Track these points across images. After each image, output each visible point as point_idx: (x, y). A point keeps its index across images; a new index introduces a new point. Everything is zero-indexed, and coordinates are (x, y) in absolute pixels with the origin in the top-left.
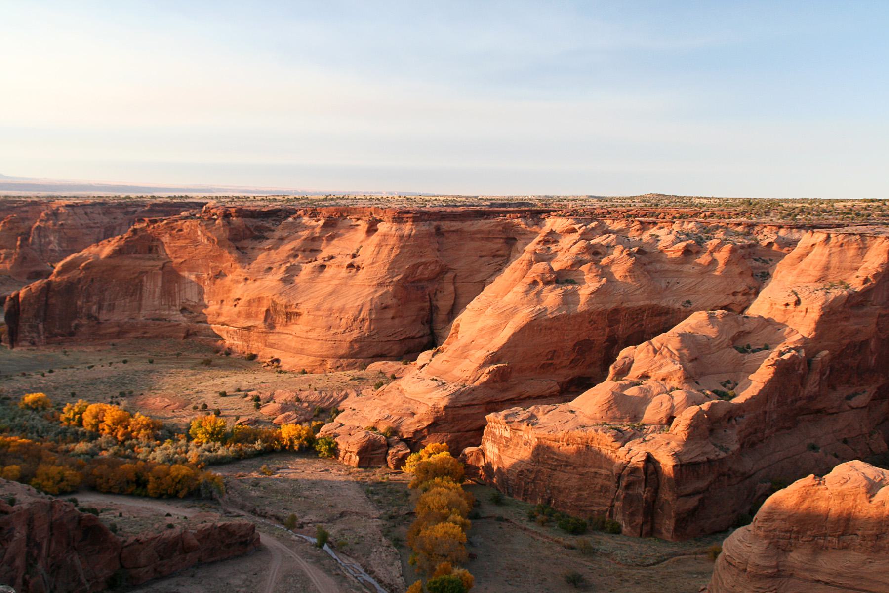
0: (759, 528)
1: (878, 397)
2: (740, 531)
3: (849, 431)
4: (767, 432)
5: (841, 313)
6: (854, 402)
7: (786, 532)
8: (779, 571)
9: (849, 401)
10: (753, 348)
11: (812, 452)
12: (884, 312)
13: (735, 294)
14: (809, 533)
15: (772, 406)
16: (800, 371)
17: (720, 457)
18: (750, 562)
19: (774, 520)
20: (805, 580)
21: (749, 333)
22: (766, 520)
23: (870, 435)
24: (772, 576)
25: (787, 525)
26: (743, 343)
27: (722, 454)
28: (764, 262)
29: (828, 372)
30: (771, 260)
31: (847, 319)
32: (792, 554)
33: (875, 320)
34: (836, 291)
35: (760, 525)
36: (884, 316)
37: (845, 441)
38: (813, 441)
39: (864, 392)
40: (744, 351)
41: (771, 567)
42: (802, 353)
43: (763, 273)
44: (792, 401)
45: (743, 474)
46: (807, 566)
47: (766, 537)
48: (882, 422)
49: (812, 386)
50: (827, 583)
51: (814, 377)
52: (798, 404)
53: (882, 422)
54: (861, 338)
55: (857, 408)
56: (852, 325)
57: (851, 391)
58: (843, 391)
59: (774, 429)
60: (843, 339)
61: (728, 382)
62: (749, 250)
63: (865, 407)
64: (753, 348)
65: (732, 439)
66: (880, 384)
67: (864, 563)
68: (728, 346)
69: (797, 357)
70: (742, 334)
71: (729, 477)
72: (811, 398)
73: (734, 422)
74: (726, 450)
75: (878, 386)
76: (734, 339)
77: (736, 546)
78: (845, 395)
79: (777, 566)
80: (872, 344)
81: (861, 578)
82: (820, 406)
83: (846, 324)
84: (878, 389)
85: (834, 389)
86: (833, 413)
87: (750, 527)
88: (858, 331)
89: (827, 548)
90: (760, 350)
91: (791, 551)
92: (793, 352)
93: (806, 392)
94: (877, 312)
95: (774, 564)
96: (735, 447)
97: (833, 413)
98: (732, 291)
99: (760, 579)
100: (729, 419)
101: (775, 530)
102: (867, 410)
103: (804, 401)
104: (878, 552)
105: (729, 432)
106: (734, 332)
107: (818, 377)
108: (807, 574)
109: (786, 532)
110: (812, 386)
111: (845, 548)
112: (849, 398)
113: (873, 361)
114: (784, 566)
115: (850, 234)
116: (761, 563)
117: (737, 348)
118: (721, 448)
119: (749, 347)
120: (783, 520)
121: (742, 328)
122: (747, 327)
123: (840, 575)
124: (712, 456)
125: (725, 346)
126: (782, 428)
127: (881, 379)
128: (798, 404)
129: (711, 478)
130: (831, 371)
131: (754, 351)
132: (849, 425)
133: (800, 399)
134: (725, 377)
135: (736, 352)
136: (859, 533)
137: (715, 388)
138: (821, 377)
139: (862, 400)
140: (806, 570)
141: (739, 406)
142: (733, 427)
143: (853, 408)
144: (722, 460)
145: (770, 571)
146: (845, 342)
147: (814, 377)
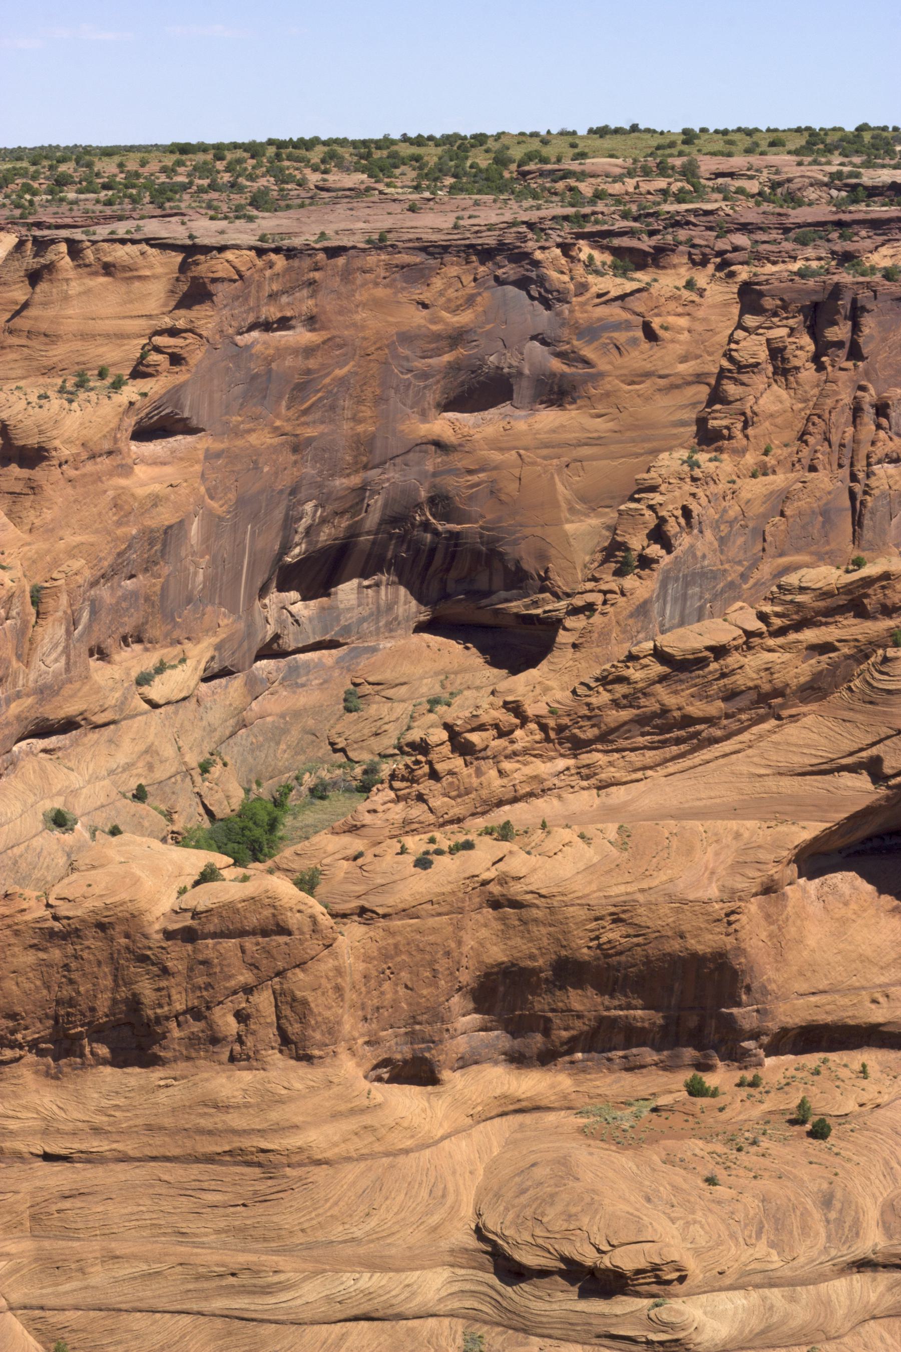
3: (150, 767)
5: (110, 453)
6: (157, 691)
9: (145, 689)
11: (57, 833)
12: (219, 446)
23: (205, 768)
29: (85, 616)
36: (218, 455)
37: (140, 795)
38: (58, 803)
39: (183, 661)
48: (233, 734)
49: (48, 662)
53: (233, 734)
54: (165, 516)
57: (150, 661)
60: (119, 524)
66: (222, 634)
72: (45, 692)
75: (215, 640)
78: (134, 674)
80: (195, 529)
82: (70, 709)
83: (123, 482)
84: (219, 647)
88: (156, 501)
93: (32, 676)
102: (193, 700)
103: (30, 701)
107: (61, 631)
112: (143, 680)
113: (200, 577)
127: (223, 622)
128: (15, 708)
130: (94, 612)
132: (146, 752)
133: (18, 696)
138: (68, 633)
143: (155, 705)
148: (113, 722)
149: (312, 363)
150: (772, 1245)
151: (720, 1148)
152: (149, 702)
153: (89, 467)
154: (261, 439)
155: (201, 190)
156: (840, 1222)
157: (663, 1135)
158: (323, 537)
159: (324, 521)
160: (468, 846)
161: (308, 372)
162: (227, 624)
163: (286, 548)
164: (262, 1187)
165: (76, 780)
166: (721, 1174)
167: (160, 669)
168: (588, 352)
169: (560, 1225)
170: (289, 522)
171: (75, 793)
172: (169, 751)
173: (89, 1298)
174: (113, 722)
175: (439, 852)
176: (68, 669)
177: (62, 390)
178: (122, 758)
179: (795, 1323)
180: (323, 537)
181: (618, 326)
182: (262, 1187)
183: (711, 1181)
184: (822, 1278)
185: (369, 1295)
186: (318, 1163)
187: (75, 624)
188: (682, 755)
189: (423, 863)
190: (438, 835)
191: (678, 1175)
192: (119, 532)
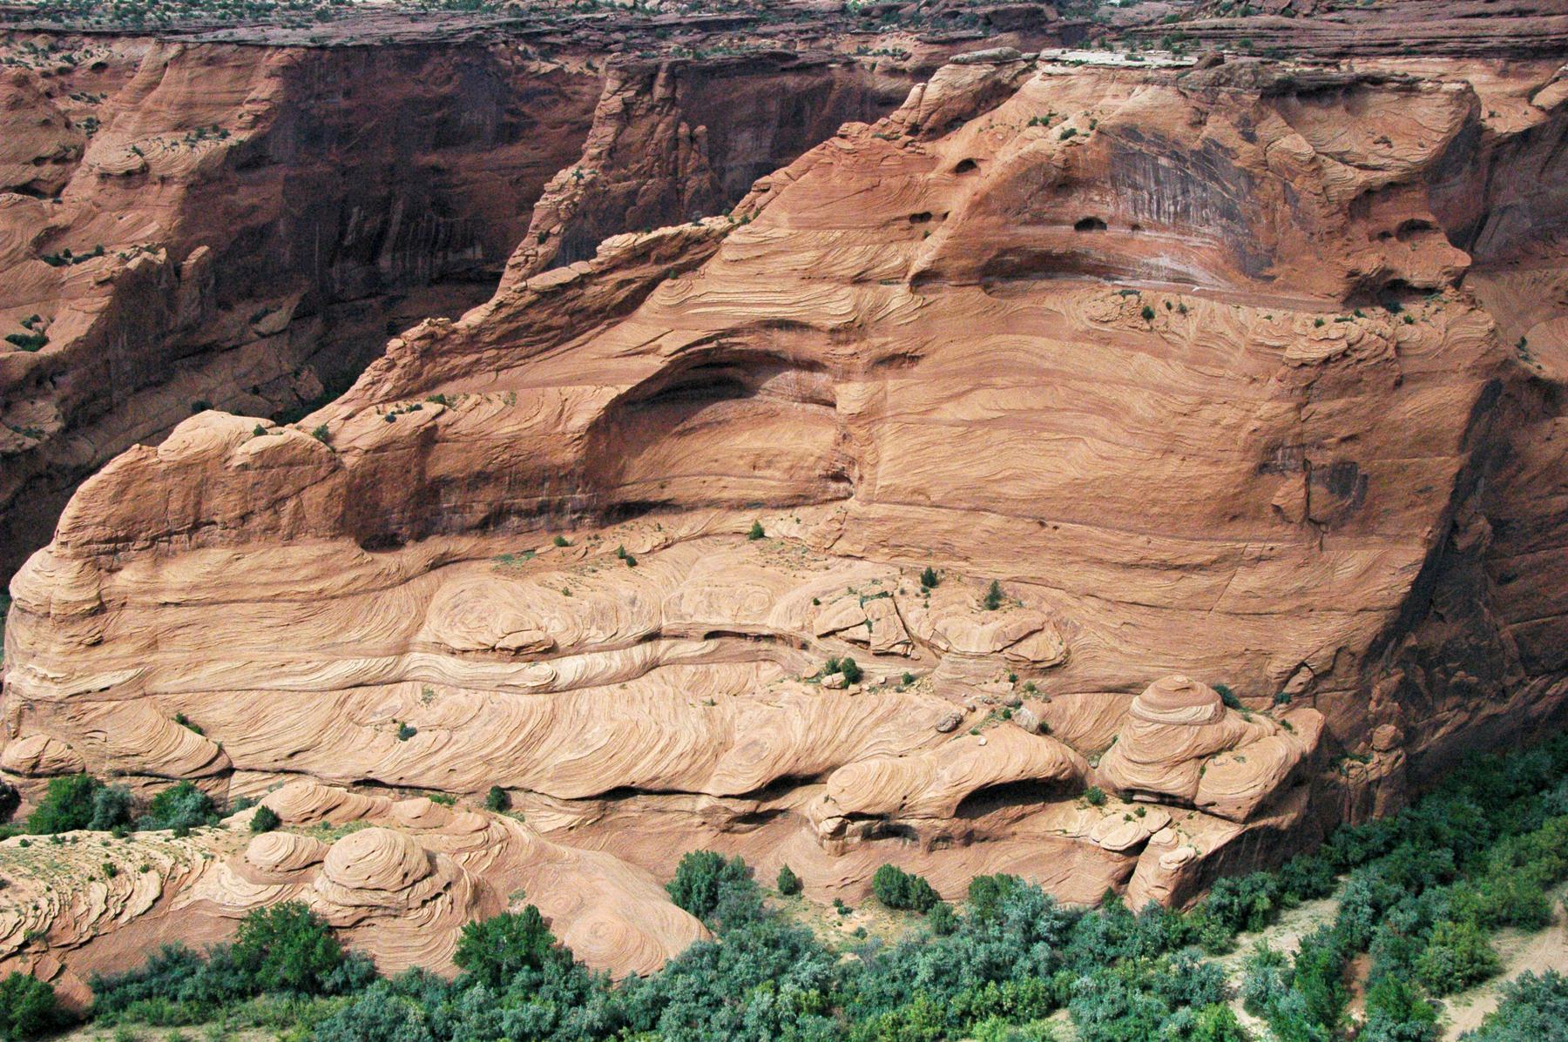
0: (64, 544)
1: (302, 315)
2: (37, 559)
4: (116, 395)
5: (220, 179)
6: (264, 326)
7: (108, 541)
8: (102, 604)
10: (75, 254)
13: (39, 161)
14: (143, 535)
15: (119, 350)
16: (164, 285)
17: (26, 447)
18: (54, 600)
19: (85, 527)
20: (145, 606)
21: (66, 229)
22: (73, 530)
23: (297, 373)
24: (94, 613)
25: (108, 531)
26: (58, 248)
27: (30, 442)
28: (92, 100)
29: (212, 282)
30: (104, 97)
31: (234, 191)
32: (121, 573)
33: (280, 188)
34: (207, 143)
35: (64, 539)
36: (294, 178)
37: (256, 391)
40: (58, 262)
41: (90, 601)
42: (162, 255)
43: (90, 120)
44: (157, 338)
45: (78, 468)
46: (146, 587)
47: (76, 556)
49: (188, 310)
50: (178, 605)
51: (188, 294)
52: (169, 341)
54: (260, 219)
55: (272, 334)
56: (244, 198)
57: (260, 307)
58: (244, 310)
59: (131, 389)
60: (231, 223)
61: (36, 319)
62: (62, 78)
63: (282, 331)
64: (75, 254)
65: (46, 415)
67: (229, 562)
68: (29, 256)
69: (153, 263)
70: (54, 233)
71: (50, 477)
72: (188, 329)
73: (49, 385)
74: (38, 434)
76: (39, 244)
77: (31, 582)
79: (99, 597)
81: (228, 585)
82: (205, 340)
84: (302, 299)
85: (226, 306)
86: (230, 349)
87: (53, 546)
88: (253, 208)
89: (174, 553)
90: (90, 256)
91: (120, 569)
92: (146, 254)
94: (282, 174)
95: (94, 593)
96: (53, 427)
97: (230, 349)
98: (32, 157)
99: (73, 623)
100: (39, 383)
101: (88, 543)
104: (247, 541)
105: (40, 404)
106: (35, 232)
107: (196, 292)
108: (148, 599)
109: (108, 541)
110: (188, 310)
111: (201, 546)
112: (256, 319)
114: (109, 594)
115: (221, 43)
116: (74, 597)
117: (46, 259)
118: (29, 433)
119: (68, 254)
120: (98, 524)
121: (52, 222)
122: (60, 220)
123: (196, 587)
124: (11, 448)
125: (22, 256)
126: (147, 385)
127: (305, 283)
128: (169, 341)
129: (16, 484)
131: (78, 261)
134: (30, 311)
135: (46, 265)
136: (217, 519)
137: (12, 332)
139: (278, 319)
140: (145, 592)
141: (55, 359)
142: (48, 394)
143: (263, 336)
144: (32, 451)
145: (88, 607)
146: (238, 227)
147: (188, 294)
148: (236, 347)
149: (351, 120)
150: (600, 628)
151: (572, 575)
152: (258, 333)
153: (212, 188)
154: (319, 168)
155: (285, 9)
156: (639, 613)
157: (540, 569)
158: (367, 227)
159: (366, 218)
160: (418, 408)
161: (349, 125)
162: (306, 285)
163: (342, 235)
164: (298, 614)
165: (212, 383)
166: (571, 589)
167: (266, 313)
168: (526, 109)
169: (475, 624)
170: (344, 219)
171: (212, 391)
172: (274, 364)
173: (196, 685)
174: (236, 347)
175: (401, 412)
176: (202, 315)
177: (187, 139)
178: (243, 369)
179: (612, 671)
180: (367, 227)
181: (544, 92)
182: (298, 614)
183: (567, 593)
184: (629, 645)
185: (366, 672)
186: (333, 598)
187: (206, 286)
188: (547, 349)
189: (391, 419)
190: (400, 403)
191: (547, 592)
192: (232, 229)
